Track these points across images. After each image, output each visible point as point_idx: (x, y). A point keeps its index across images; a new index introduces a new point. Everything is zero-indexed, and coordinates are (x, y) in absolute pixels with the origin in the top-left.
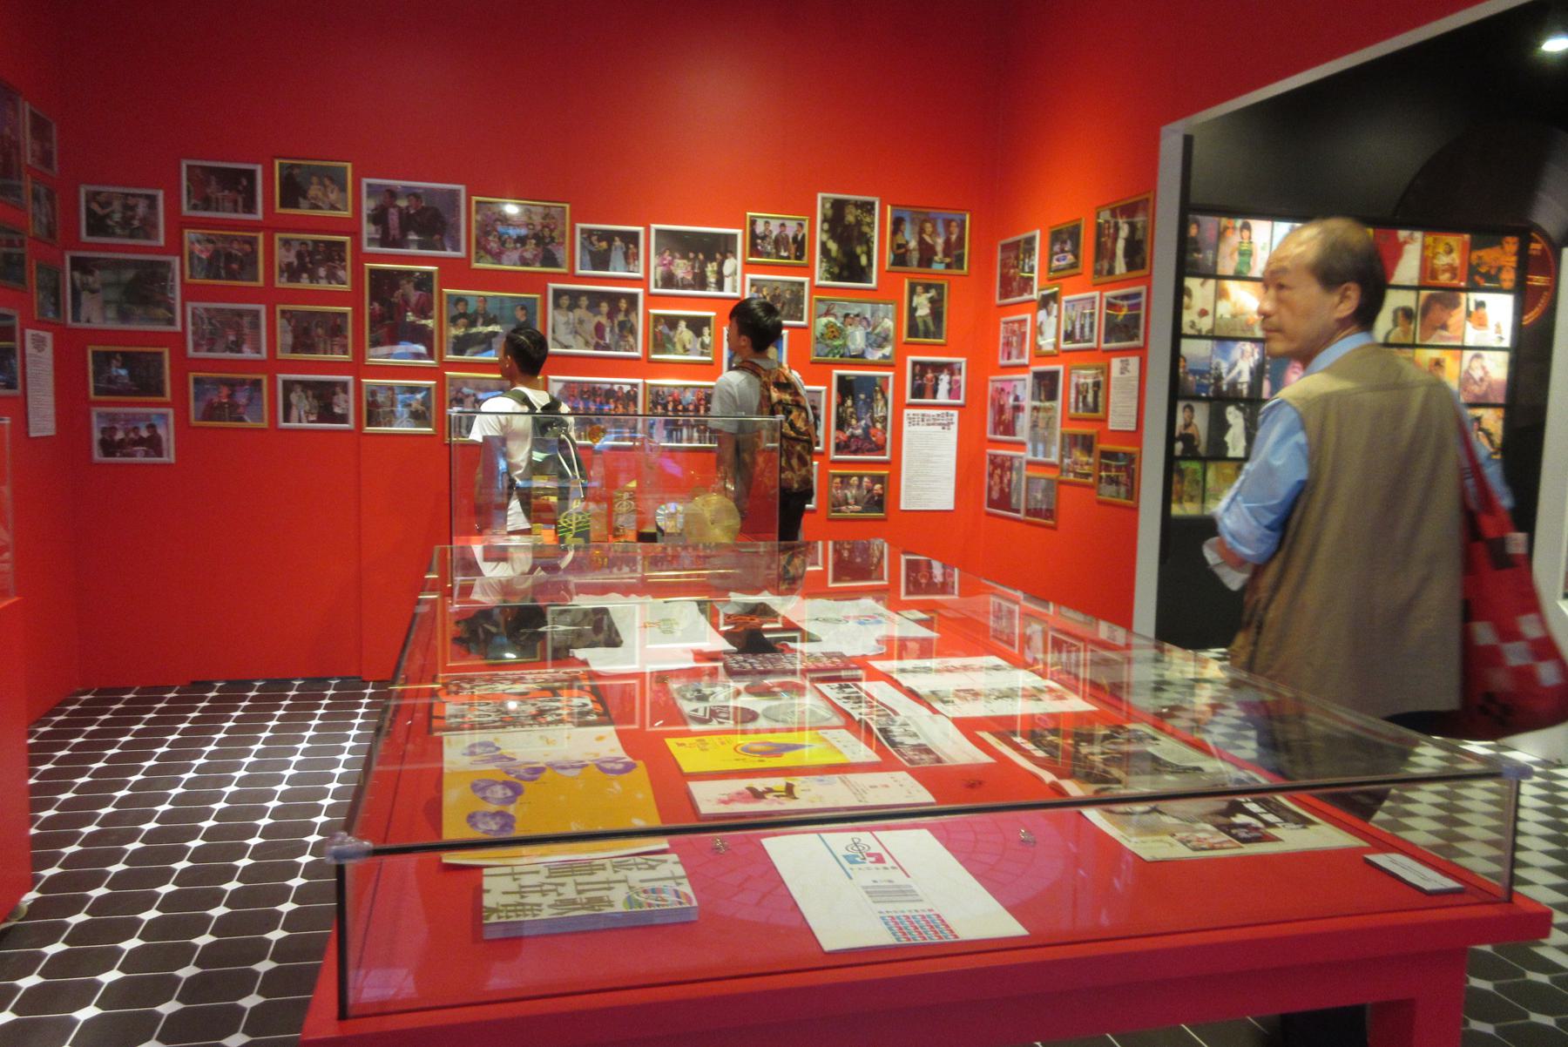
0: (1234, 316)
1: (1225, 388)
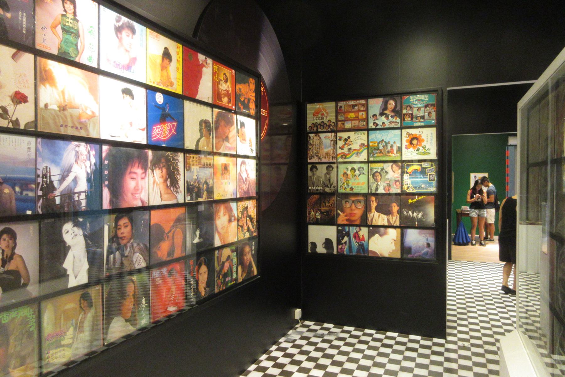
0: (63, 108)
1: (58, 200)
